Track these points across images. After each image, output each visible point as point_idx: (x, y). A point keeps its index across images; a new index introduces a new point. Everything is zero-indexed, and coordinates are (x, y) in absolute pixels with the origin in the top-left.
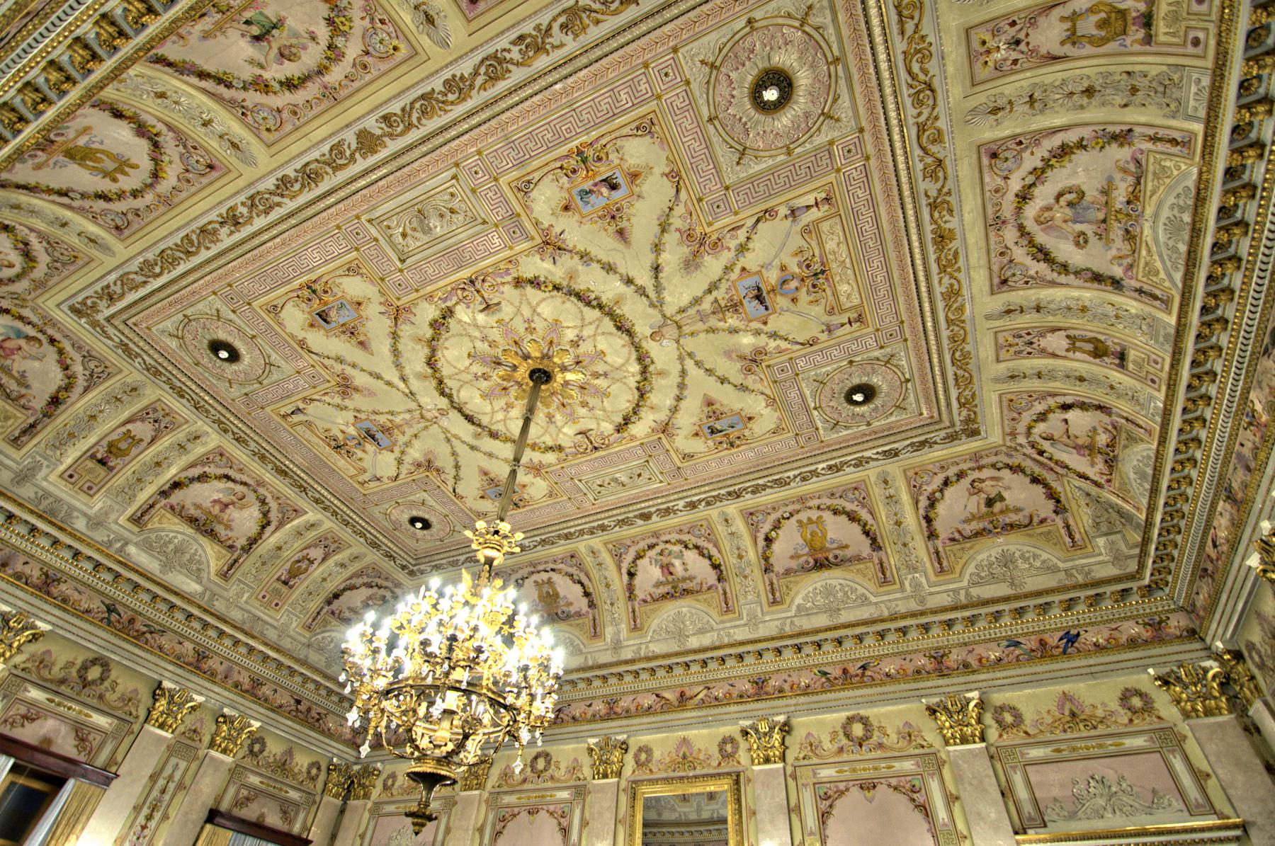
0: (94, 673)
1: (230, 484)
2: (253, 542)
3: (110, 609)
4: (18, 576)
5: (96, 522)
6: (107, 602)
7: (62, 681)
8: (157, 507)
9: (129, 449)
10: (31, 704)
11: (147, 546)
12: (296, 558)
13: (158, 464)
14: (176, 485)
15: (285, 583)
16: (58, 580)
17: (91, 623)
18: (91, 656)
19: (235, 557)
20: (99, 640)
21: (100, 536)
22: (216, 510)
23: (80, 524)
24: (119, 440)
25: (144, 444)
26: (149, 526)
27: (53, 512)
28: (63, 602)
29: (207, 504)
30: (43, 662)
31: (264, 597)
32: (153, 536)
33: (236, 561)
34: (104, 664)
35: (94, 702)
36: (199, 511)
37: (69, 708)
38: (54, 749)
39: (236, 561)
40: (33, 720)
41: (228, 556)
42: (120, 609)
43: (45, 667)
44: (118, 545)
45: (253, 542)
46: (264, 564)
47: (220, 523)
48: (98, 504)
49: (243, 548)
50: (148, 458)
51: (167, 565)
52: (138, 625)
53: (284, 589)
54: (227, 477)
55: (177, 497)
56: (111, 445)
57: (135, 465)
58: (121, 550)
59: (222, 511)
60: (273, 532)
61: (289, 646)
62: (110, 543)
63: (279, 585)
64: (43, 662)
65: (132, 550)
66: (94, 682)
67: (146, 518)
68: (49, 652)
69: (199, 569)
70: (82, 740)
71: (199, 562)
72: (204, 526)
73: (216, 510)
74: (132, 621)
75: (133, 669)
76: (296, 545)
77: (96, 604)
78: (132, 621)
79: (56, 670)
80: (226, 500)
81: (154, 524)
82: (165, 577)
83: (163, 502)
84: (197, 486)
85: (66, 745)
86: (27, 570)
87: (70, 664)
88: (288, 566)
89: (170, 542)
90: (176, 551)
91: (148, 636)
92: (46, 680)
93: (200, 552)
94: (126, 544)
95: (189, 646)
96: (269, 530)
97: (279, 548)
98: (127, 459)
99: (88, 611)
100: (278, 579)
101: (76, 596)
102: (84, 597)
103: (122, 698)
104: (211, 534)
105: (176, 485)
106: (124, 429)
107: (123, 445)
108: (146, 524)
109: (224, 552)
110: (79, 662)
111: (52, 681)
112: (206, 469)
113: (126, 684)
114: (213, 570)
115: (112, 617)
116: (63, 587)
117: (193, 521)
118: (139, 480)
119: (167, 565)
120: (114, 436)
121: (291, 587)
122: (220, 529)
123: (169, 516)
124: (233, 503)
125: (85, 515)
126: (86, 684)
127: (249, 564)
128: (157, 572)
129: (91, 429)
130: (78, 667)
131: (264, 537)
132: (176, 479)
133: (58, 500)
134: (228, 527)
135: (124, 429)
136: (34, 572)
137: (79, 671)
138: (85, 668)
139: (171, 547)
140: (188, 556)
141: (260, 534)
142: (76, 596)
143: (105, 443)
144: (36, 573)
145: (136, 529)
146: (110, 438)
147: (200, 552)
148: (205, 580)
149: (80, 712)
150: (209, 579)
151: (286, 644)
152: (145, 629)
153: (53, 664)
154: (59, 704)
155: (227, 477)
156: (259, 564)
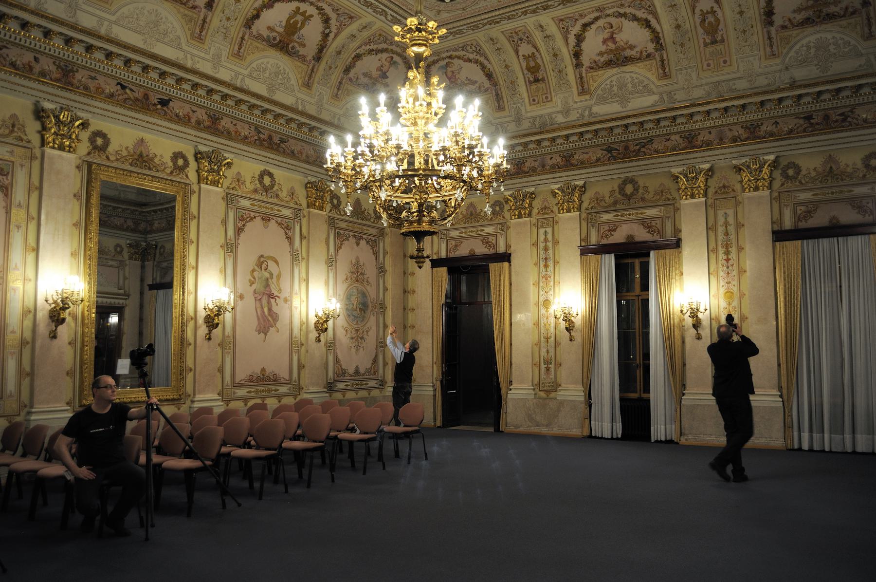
0: (629, 189)
1: (594, 27)
2: (657, 39)
3: (609, 150)
4: (553, 167)
5: (566, 112)
6: (604, 147)
7: (615, 203)
8: (584, 75)
9: (536, 63)
10: (608, 222)
11: (602, 100)
12: (698, 21)
13: (555, 55)
14: (577, 55)
15: (714, 42)
16: (572, 155)
17: (604, 165)
18: (620, 181)
19: (658, 59)
20: (617, 172)
21: (574, 116)
22: (612, 46)
23: (560, 119)
24: (528, 63)
25: (537, 54)
26: (592, 89)
27: (544, 124)
28: (582, 165)
29: (603, 48)
30: (598, 199)
31: (709, 65)
32: (599, 92)
33: (662, 61)
34: (632, 181)
35: (641, 204)
36: (605, 56)
37: (630, 215)
38: (637, 239)
39: (662, 61)
40: (615, 230)
41: (654, 63)
42: (614, 146)
43: (601, 201)
44: (587, 113)
45: (657, 39)
46: (682, 45)
47: (624, 49)
48: (558, 100)
49: (657, 50)
50: (548, 58)
51: (623, 101)
52: (632, 148)
53: (719, 47)
54: (585, 26)
55: (586, 60)
56: (529, 69)
57: (549, 67)
58: (590, 114)
59: (615, 43)
60: (659, 22)
61: (766, 82)
62: (582, 116)
63: (711, 48)
64: (598, 199)
65: (595, 109)
66: (632, 194)
67: (586, 86)
68: (597, 193)
69: (644, 86)
70: (649, 227)
71: (641, 82)
72: (618, 58)
73: (612, 46)
74: (626, 148)
75: (650, 173)
76: (684, 14)
77: (599, 153)
78: (626, 148)
79: (607, 199)
80: (606, 35)
81: (593, 86)
82: (628, 108)
83: (583, 70)
84: (584, 46)
85: (642, 235)
86: (554, 161)
87: (612, 192)
88: (700, 31)
89: (612, 86)
90: (620, 88)
91: (643, 149)
92: (606, 207)
93: (634, 76)
94: (591, 108)
95: (676, 137)
96: (653, 22)
97: (678, 27)
98: (542, 67)
99: (598, 160)
100: (706, 45)
101: (586, 156)
102: (590, 154)
103: (656, 193)
104: (628, 60)
105: (577, 55)
106: (521, 58)
107: (532, 64)
108: (589, 89)
109: (648, 63)
110: (616, 188)
111: (609, 206)
112: (573, 33)
113: (653, 185)
114: (653, 78)
115: (618, 153)
116: (576, 157)
117: (609, 64)
118: (560, 71)
119: (623, 101)
120: (524, 65)
121: (723, 41)
122: (628, 53)
123: (596, 73)
124: (613, 33)
125: (558, 112)
126: (629, 197)
127: (672, 54)
128: (621, 109)
129: (513, 72)
130: (617, 191)
131: (658, 29)
132: (572, 53)
133: (541, 116)
134: (631, 47)
135: (521, 58)
136: (557, 159)
137: (620, 193)
138: (622, 189)
139: (615, 88)
140: (630, 85)
141: (653, 31)
142: (586, 156)
143: (526, 72)
144: (559, 159)
145: (587, 97)
146: (524, 67)
147: (634, 76)
148: (655, 90)
149: (637, 214)
150: (657, 87)
151: (762, 81)
152: (638, 147)
153: (604, 197)
154: (622, 215)
155: (585, 26)
156: (679, 49)
